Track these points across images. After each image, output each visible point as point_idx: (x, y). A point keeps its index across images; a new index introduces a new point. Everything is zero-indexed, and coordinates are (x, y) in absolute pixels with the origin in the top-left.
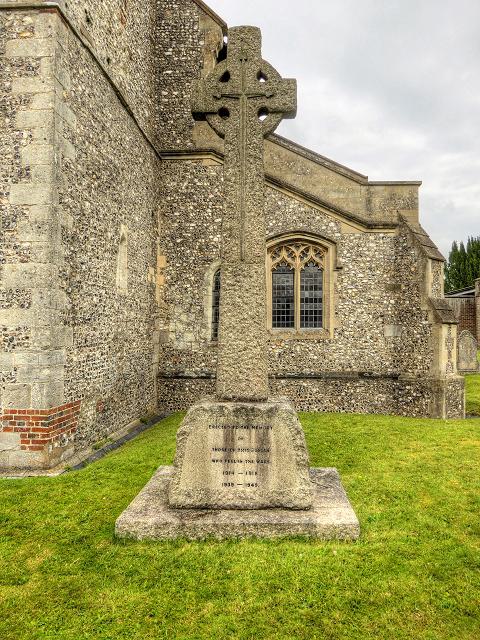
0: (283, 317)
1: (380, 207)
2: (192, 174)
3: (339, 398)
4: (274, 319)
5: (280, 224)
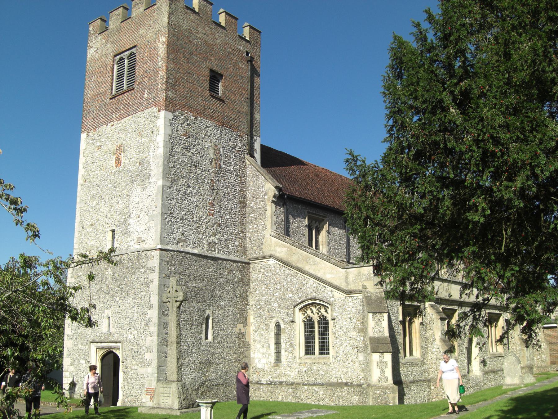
0: (309, 350)
1: (353, 281)
2: (264, 269)
3: (334, 398)
4: (306, 350)
5: (304, 295)
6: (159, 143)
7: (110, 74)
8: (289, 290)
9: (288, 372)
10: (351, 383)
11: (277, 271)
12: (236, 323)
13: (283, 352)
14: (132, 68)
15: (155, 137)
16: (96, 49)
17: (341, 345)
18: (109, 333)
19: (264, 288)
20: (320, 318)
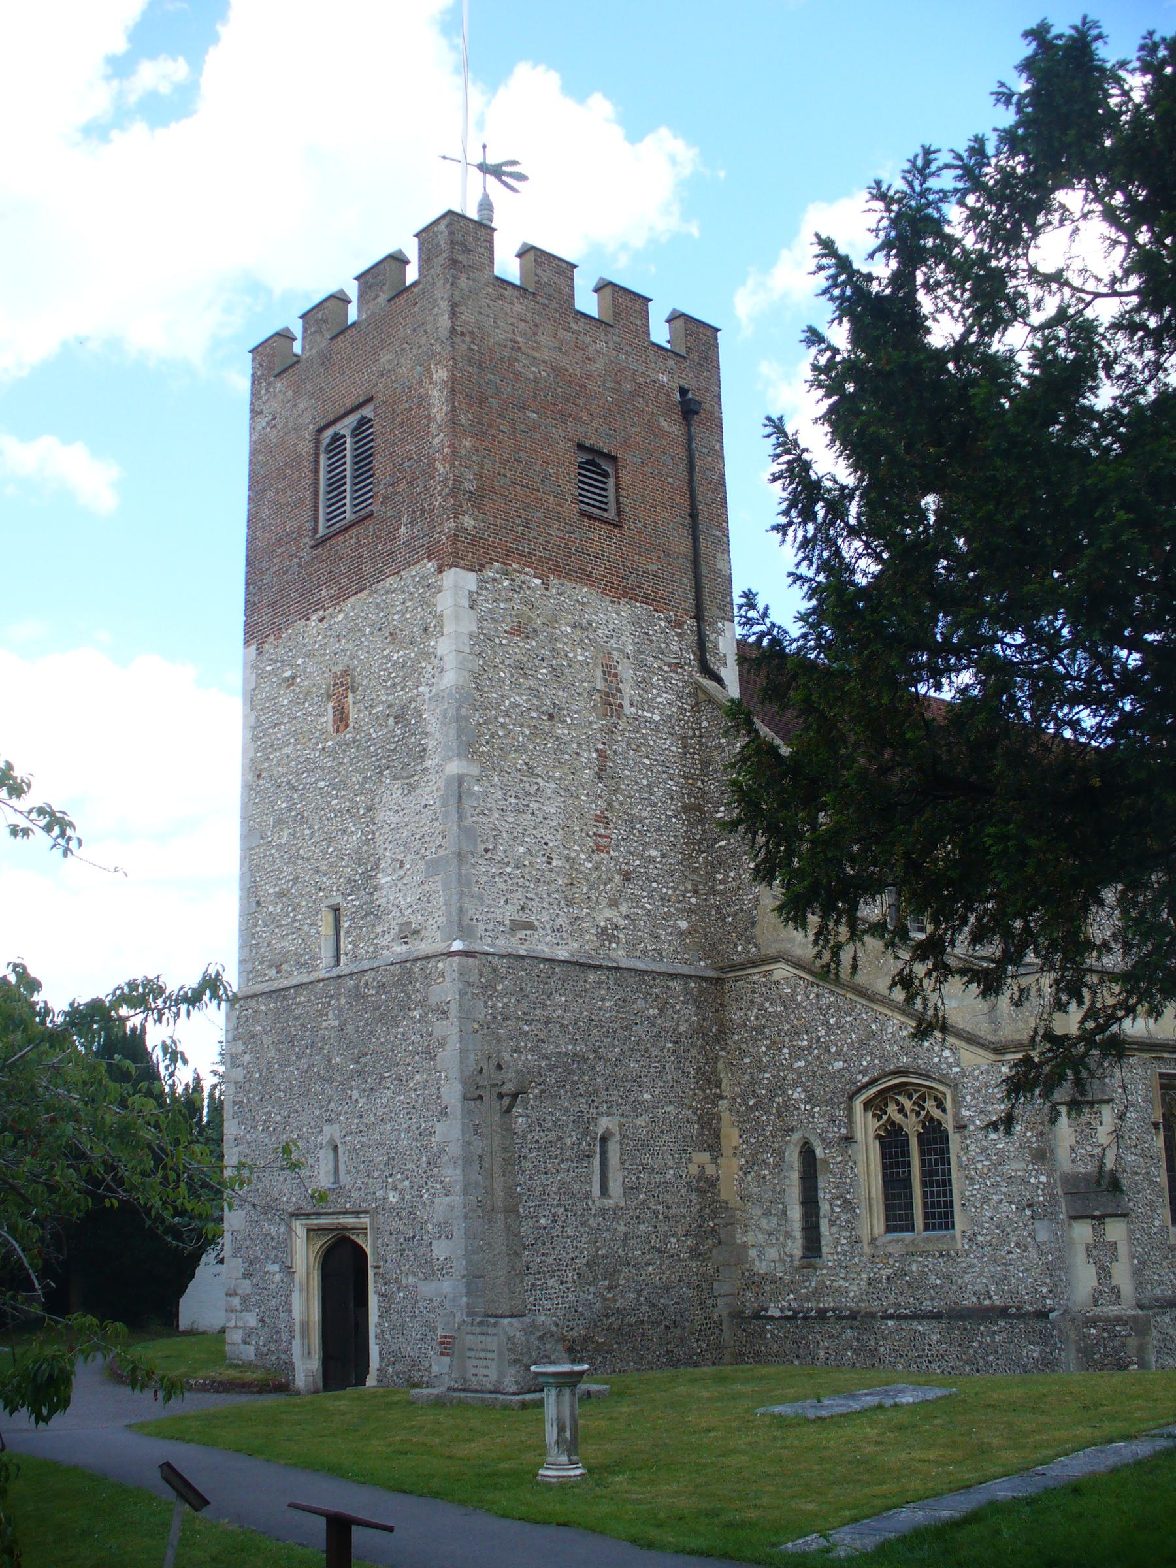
2: (762, 995)
3: (971, 1351)
4: (887, 1219)
5: (876, 1061)
6: (446, 658)
7: (310, 482)
8: (833, 1050)
9: (842, 1282)
10: (1018, 1309)
11: (799, 998)
12: (690, 1150)
13: (824, 1225)
14: (364, 461)
15: (432, 643)
16: (270, 418)
17: (986, 1200)
18: (337, 1189)
19: (764, 1049)
20: (924, 1126)
